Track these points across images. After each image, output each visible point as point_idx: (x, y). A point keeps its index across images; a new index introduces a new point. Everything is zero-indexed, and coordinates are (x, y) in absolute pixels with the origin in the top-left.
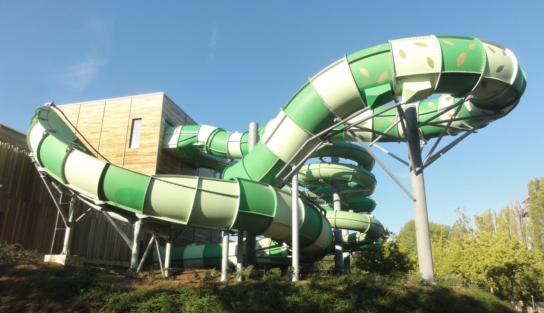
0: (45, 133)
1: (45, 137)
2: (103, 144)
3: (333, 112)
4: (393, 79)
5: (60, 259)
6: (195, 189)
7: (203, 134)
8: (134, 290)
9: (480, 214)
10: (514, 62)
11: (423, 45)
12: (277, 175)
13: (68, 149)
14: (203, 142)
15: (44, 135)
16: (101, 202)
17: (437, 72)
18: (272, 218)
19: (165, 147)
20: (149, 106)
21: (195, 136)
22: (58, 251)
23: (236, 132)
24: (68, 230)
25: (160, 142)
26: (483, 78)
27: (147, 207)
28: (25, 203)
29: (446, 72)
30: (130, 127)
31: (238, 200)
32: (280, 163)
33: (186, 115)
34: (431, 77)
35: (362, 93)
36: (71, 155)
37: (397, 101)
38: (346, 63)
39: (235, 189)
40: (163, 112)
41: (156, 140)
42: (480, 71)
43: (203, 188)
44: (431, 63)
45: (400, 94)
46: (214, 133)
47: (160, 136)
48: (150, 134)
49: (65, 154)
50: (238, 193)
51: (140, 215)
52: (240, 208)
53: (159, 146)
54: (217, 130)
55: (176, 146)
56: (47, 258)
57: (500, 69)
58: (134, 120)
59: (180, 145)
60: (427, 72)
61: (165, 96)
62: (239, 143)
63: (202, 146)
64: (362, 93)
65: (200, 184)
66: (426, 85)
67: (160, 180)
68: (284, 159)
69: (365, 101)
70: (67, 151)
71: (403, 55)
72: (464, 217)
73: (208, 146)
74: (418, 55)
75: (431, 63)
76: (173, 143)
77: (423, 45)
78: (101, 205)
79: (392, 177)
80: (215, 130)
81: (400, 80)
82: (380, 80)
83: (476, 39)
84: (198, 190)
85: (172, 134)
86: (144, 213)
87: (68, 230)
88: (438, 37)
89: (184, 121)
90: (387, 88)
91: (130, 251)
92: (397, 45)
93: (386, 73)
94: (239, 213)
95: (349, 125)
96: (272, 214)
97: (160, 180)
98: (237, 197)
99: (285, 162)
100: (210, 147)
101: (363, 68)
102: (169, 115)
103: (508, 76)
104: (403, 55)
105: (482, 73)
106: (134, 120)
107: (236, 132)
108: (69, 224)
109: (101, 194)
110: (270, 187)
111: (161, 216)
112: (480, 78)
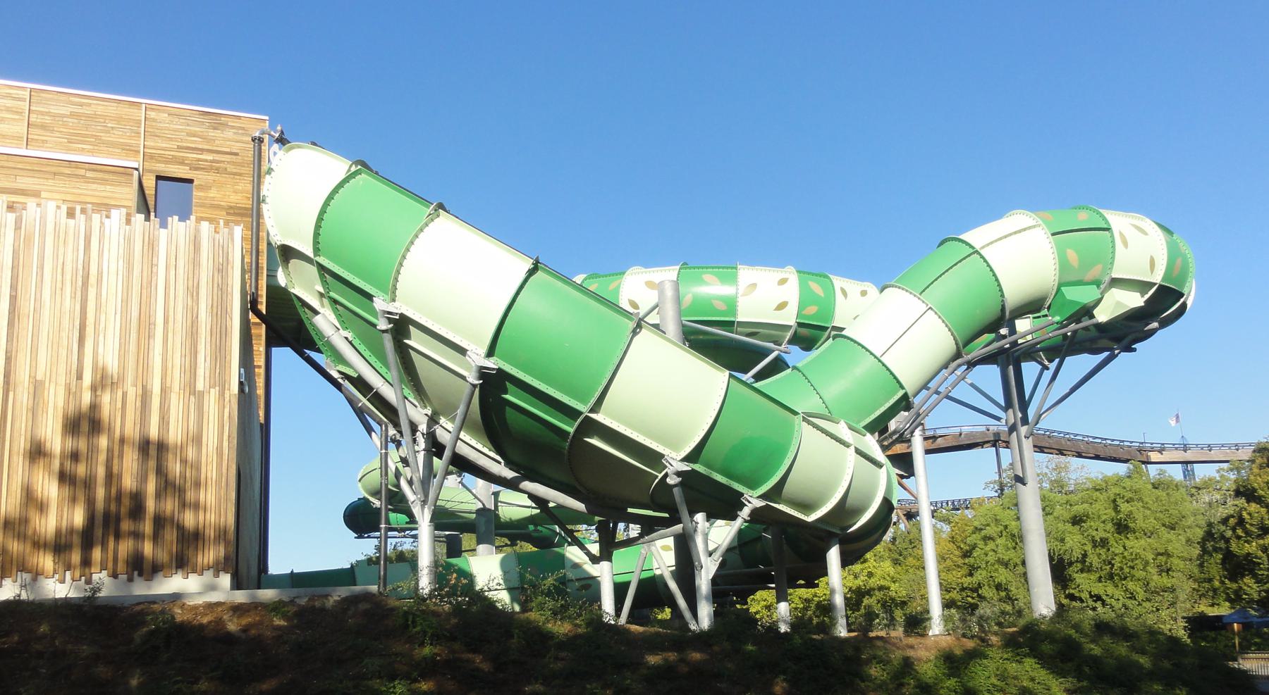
1: (531, 272)
4: (1107, 279)
16: (685, 467)
34: (1142, 286)
35: (1058, 290)
71: (1126, 244)
74: (1140, 249)
78: (679, 474)
81: (1116, 282)
82: (1089, 276)
93: (1100, 266)
104: (1126, 244)
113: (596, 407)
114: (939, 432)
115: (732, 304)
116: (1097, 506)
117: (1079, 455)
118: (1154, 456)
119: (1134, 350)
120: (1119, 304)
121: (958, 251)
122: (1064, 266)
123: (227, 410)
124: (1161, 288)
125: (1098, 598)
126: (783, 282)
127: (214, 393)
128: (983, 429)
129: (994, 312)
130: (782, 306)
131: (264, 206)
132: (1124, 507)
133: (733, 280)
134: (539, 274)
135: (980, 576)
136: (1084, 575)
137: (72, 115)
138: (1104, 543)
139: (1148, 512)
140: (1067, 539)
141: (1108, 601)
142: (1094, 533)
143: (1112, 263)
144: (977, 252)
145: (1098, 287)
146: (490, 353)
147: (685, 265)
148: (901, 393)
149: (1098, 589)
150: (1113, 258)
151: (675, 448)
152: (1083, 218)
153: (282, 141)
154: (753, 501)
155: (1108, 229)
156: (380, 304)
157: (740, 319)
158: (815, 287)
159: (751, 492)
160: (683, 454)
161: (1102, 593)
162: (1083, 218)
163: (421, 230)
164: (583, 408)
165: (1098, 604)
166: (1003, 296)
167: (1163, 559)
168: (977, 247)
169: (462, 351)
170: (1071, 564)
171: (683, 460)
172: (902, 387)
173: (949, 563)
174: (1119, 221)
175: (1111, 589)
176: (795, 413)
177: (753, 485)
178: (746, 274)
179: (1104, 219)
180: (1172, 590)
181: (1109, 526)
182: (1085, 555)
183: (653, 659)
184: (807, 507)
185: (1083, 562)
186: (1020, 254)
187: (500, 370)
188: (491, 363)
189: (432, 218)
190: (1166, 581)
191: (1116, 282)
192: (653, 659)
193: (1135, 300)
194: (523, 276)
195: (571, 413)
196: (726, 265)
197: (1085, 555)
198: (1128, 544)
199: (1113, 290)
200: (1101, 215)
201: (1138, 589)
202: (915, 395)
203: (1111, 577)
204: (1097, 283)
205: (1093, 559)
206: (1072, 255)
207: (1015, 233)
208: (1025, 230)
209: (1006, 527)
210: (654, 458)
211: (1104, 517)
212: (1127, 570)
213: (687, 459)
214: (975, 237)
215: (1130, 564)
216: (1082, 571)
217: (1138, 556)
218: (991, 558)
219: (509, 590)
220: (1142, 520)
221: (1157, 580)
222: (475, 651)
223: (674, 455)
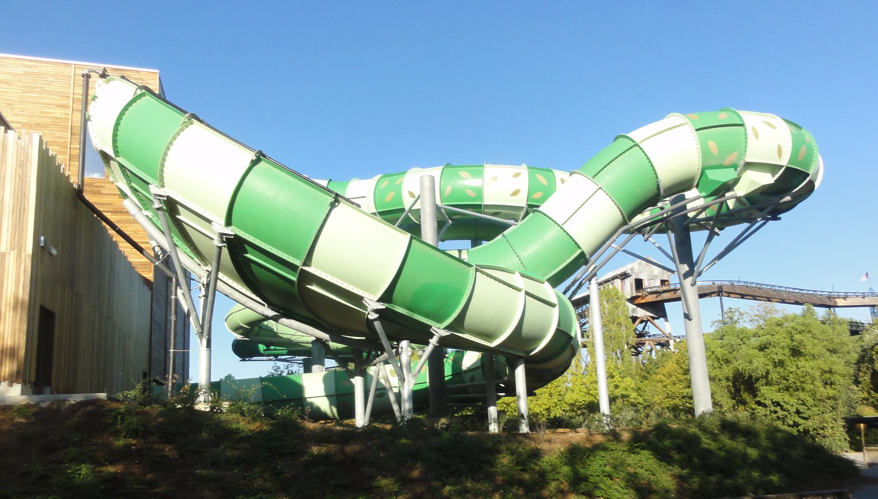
0: (255, 158)
1: (254, 163)
4: (742, 163)
11: (773, 127)
16: (381, 306)
35: (703, 173)
36: (334, 211)
71: (756, 136)
74: (768, 141)
77: (773, 127)
78: (376, 311)
81: (749, 165)
82: (727, 161)
88: (788, 122)
97: (491, 277)
104: (756, 136)
112: (808, 179)
113: (308, 261)
115: (479, 192)
116: (777, 336)
117: (783, 302)
118: (840, 302)
119: (780, 219)
120: (752, 182)
121: (624, 144)
122: (706, 154)
123: (22, 267)
124: (789, 170)
125: (777, 404)
126: (517, 175)
127: (13, 254)
128: (711, 283)
129: (651, 190)
130: (515, 193)
131: (89, 123)
132: (797, 337)
133: (480, 175)
134: (262, 165)
136: (768, 387)
137: (25, 73)
138: (781, 363)
139: (816, 341)
140: (754, 361)
141: (785, 406)
142: (774, 356)
143: (745, 151)
144: (637, 145)
145: (736, 170)
146: (229, 223)
147: (448, 165)
149: (778, 397)
150: (746, 147)
151: (371, 290)
152: (723, 117)
153: (104, 75)
154: (439, 331)
155: (742, 125)
156: (154, 189)
157: (485, 203)
158: (541, 178)
159: (438, 325)
160: (378, 296)
161: (780, 400)
162: (723, 117)
164: (298, 262)
165: (778, 409)
166: (657, 177)
167: (828, 375)
168: (638, 142)
169: (209, 221)
170: (757, 380)
171: (379, 301)
172: (579, 247)
173: (674, 378)
174: (750, 118)
175: (787, 398)
176: (470, 266)
177: (439, 320)
178: (490, 170)
179: (740, 117)
180: (834, 398)
181: (787, 351)
182: (768, 373)
183: (315, 450)
184: (490, 336)
185: (766, 377)
186: (671, 147)
187: (235, 236)
188: (229, 231)
189: (185, 125)
190: (831, 392)
191: (749, 165)
192: (315, 450)
193: (767, 179)
194: (247, 165)
195: (292, 267)
196: (475, 164)
197: (768, 373)
198: (799, 363)
199: (748, 171)
200: (738, 115)
201: (808, 398)
202: (592, 254)
203: (787, 389)
204: (735, 167)
205: (774, 376)
206: (712, 145)
207: (668, 130)
208: (675, 127)
209: (713, 353)
210: (357, 299)
211: (782, 344)
212: (798, 384)
213: (380, 300)
214: (637, 135)
215: (802, 379)
216: (767, 384)
217: (807, 374)
219: (328, 396)
220: (810, 346)
221: (824, 391)
222: (166, 442)
223: (372, 297)
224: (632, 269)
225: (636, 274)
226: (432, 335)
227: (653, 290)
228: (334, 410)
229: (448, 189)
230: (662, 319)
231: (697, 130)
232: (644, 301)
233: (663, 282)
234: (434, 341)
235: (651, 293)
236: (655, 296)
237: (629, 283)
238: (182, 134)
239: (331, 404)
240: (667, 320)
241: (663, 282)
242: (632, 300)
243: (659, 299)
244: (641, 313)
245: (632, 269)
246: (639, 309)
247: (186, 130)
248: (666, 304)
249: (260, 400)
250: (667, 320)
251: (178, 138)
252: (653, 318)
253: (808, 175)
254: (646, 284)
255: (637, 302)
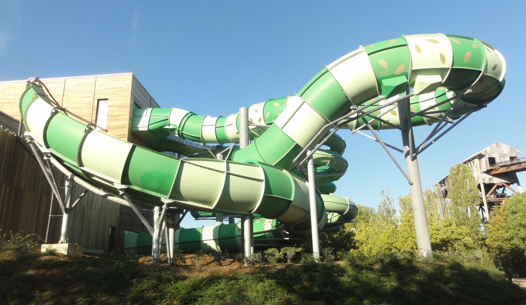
0: (54, 111)
1: (53, 114)
2: (85, 125)
3: (351, 100)
4: (409, 72)
5: (62, 248)
6: (224, 172)
7: (175, 118)
8: (184, 278)
9: (403, 197)
10: (502, 62)
11: (436, 42)
12: (295, 160)
13: (87, 129)
14: (175, 126)
15: (52, 113)
16: (124, 187)
17: (447, 67)
18: (291, 202)
19: (134, 129)
20: (117, 86)
21: (167, 119)
22: (54, 239)
23: (209, 117)
24: (65, 217)
25: (129, 124)
26: (483, 75)
27: (176, 193)
28: (8, 187)
29: (454, 67)
30: (95, 108)
31: (263, 184)
32: (297, 148)
33: (151, 97)
34: (441, 71)
35: (379, 83)
36: (89, 135)
37: (408, 93)
38: (365, 55)
39: (259, 172)
40: (132, 93)
41: (125, 122)
42: (480, 68)
43: (231, 172)
44: (443, 58)
45: (413, 85)
46: (187, 117)
47: (130, 118)
48: (119, 116)
49: (83, 134)
50: (263, 178)
51: (166, 200)
52: (266, 192)
53: (129, 129)
54: (190, 114)
55: (146, 129)
56: (44, 248)
57: (495, 68)
58: (99, 100)
59: (151, 127)
60: (439, 67)
61: (133, 76)
62: (214, 127)
63: (173, 130)
64: (379, 83)
65: (228, 168)
66: (437, 79)
67: (190, 163)
68: (301, 144)
69: (380, 90)
70: (86, 131)
71: (419, 50)
72: (388, 199)
73: (180, 129)
74: (432, 51)
75: (443, 58)
76: (143, 125)
77: (436, 42)
78: (121, 190)
79: (395, 162)
80: (188, 114)
81: (415, 72)
82: (397, 72)
83: (475, 40)
84: (227, 173)
85: (141, 116)
86: (170, 198)
87: (65, 217)
89: (149, 103)
90: (402, 80)
91: (151, 237)
92: (412, 40)
93: (403, 65)
94: (264, 197)
95: (363, 113)
96: (290, 197)
98: (262, 181)
99: (302, 146)
100: (182, 130)
101: (382, 59)
102: (137, 96)
103: (499, 74)
104: (419, 50)
105: (482, 71)
106: (99, 100)
107: (209, 117)
108: (67, 211)
109: (125, 178)
110: (285, 171)
111: (187, 201)
112: (481, 74)
114: (522, 160)
120: (421, 83)
134: (61, 114)
135: (511, 232)
148: (295, 144)
155: (406, 45)
159: (166, 196)
163: (31, 104)
194: (49, 115)
199: (418, 76)
210: (112, 183)
218: (515, 223)
219: (215, 239)
224: (485, 151)
225: (489, 154)
226: (163, 204)
227: (504, 164)
228: (219, 247)
229: (267, 114)
230: (515, 184)
231: (369, 54)
232: (497, 172)
233: (512, 158)
234: (164, 207)
235: (502, 167)
236: (505, 168)
237: (485, 160)
238: (33, 104)
239: (217, 244)
240: (519, 185)
241: (512, 158)
242: (488, 172)
243: (509, 170)
244: (497, 181)
245: (485, 151)
246: (494, 178)
247: (35, 101)
248: (518, 174)
249: (178, 242)
250: (519, 185)
251: (31, 106)
252: (509, 184)
253: (481, 72)
254: (497, 160)
255: (492, 173)
